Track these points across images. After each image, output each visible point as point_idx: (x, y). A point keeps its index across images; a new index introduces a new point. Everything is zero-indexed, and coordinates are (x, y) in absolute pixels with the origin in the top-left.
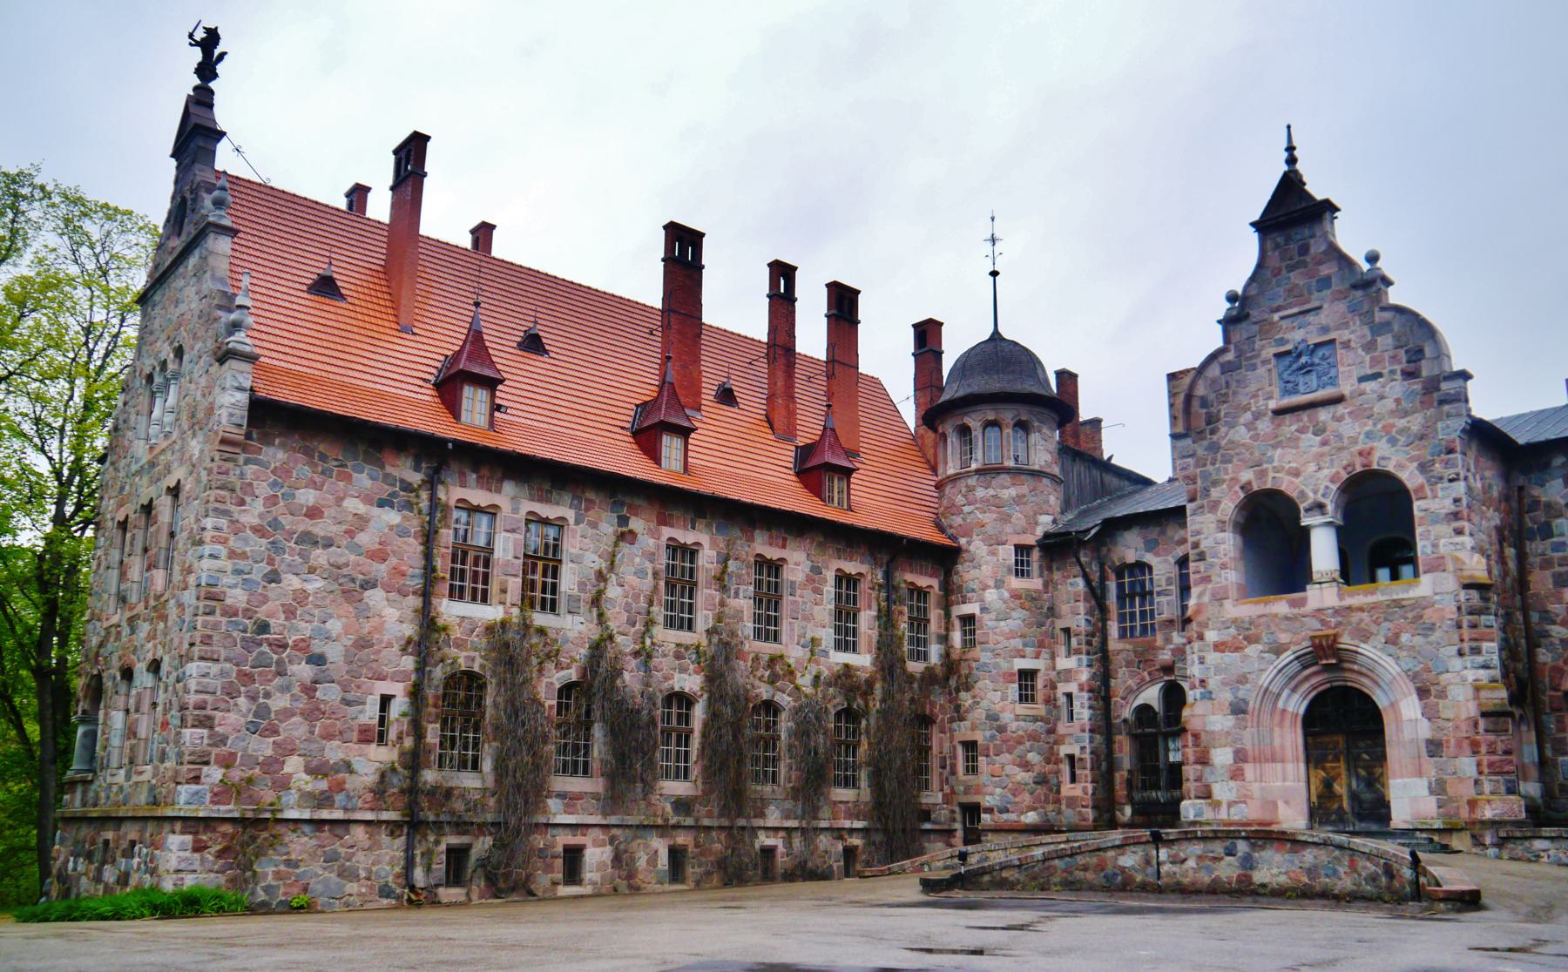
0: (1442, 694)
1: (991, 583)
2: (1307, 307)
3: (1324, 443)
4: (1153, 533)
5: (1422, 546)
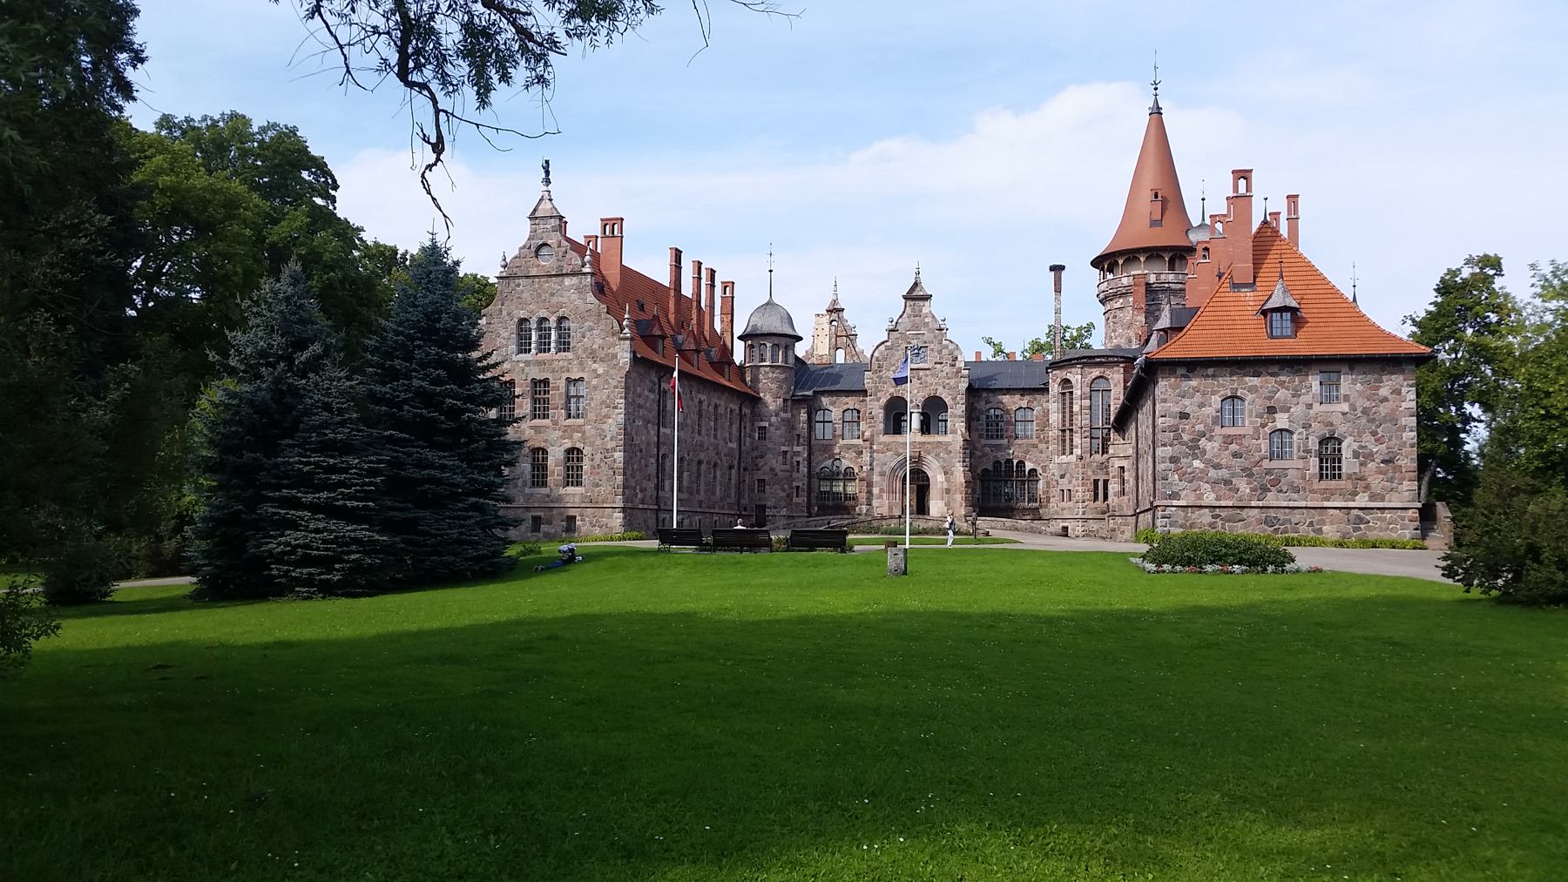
1: (774, 414)
3: (921, 384)
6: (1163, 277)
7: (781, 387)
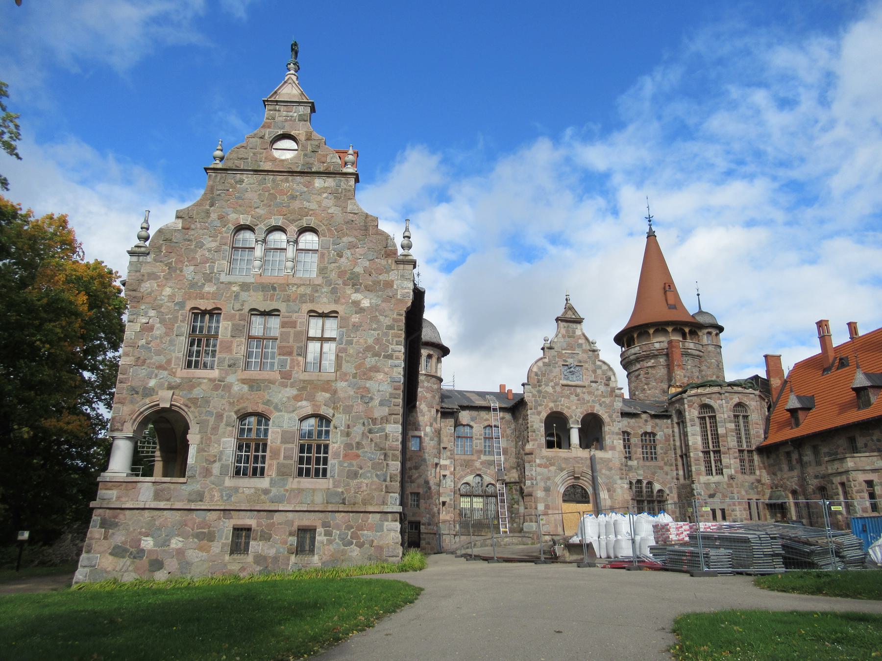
0: (614, 491)
1: (429, 424)
2: (574, 352)
3: (579, 400)
4: (474, 413)
5: (608, 440)
6: (687, 344)
7: (434, 397)
